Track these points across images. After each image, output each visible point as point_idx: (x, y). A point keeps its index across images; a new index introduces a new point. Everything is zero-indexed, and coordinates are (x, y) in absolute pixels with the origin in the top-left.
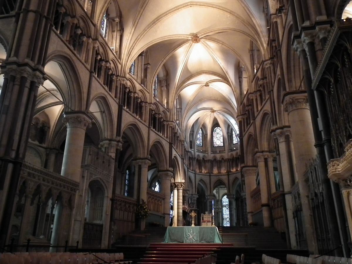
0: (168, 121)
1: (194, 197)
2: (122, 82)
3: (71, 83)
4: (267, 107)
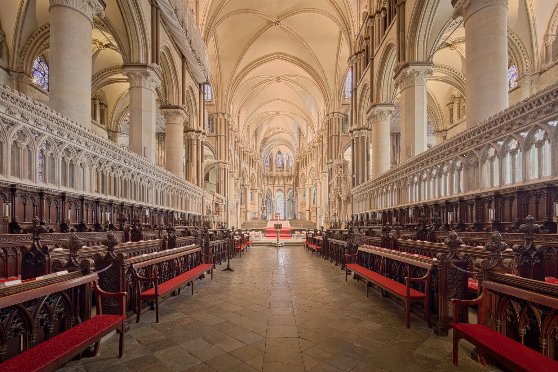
4: (314, 165)
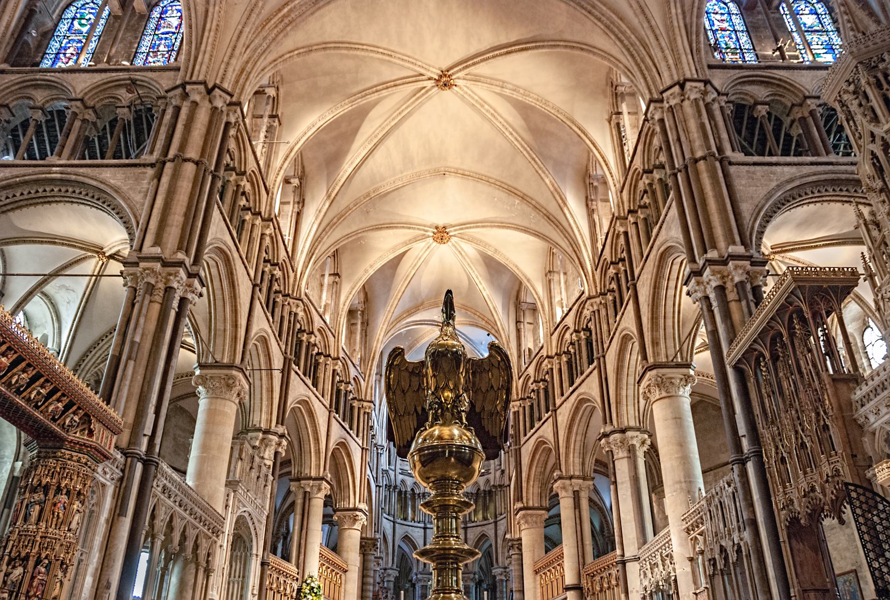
0: (362, 400)
1: (389, 575)
2: (294, 310)
3: (219, 303)
